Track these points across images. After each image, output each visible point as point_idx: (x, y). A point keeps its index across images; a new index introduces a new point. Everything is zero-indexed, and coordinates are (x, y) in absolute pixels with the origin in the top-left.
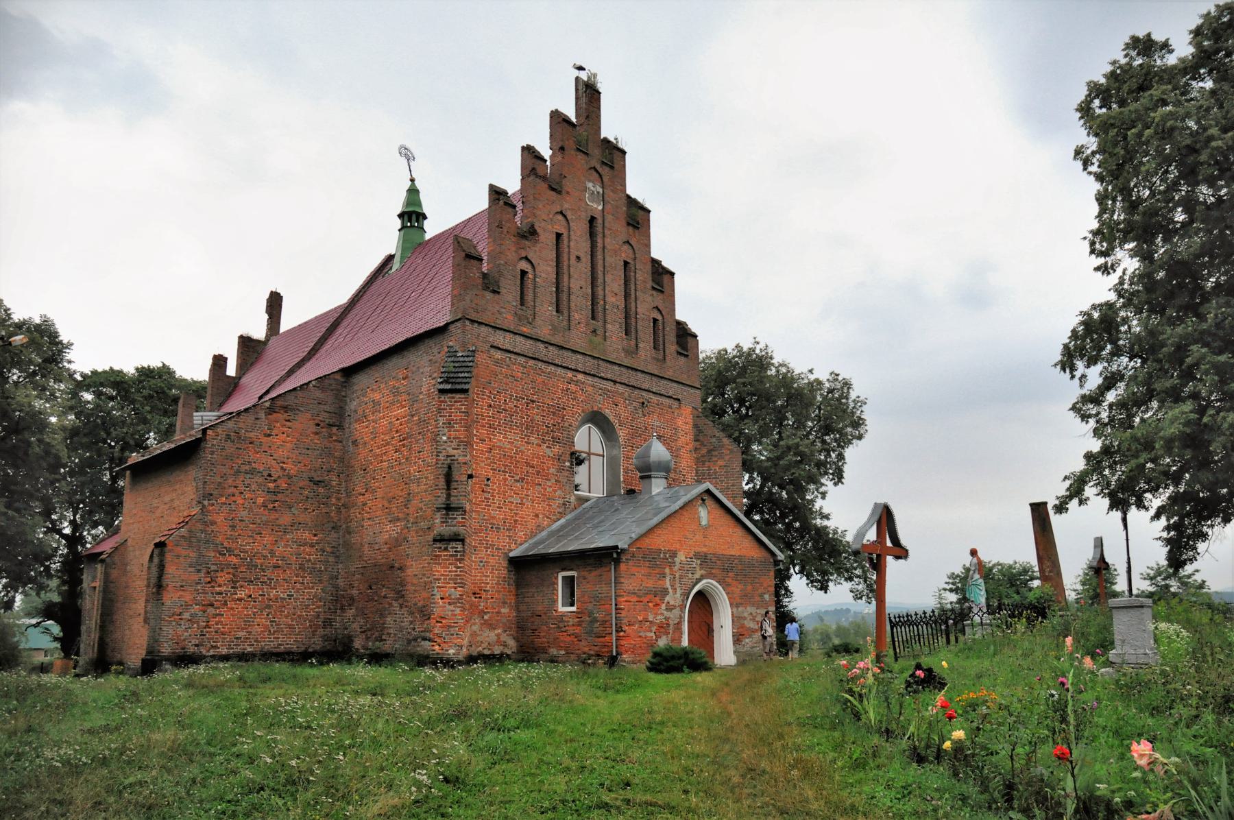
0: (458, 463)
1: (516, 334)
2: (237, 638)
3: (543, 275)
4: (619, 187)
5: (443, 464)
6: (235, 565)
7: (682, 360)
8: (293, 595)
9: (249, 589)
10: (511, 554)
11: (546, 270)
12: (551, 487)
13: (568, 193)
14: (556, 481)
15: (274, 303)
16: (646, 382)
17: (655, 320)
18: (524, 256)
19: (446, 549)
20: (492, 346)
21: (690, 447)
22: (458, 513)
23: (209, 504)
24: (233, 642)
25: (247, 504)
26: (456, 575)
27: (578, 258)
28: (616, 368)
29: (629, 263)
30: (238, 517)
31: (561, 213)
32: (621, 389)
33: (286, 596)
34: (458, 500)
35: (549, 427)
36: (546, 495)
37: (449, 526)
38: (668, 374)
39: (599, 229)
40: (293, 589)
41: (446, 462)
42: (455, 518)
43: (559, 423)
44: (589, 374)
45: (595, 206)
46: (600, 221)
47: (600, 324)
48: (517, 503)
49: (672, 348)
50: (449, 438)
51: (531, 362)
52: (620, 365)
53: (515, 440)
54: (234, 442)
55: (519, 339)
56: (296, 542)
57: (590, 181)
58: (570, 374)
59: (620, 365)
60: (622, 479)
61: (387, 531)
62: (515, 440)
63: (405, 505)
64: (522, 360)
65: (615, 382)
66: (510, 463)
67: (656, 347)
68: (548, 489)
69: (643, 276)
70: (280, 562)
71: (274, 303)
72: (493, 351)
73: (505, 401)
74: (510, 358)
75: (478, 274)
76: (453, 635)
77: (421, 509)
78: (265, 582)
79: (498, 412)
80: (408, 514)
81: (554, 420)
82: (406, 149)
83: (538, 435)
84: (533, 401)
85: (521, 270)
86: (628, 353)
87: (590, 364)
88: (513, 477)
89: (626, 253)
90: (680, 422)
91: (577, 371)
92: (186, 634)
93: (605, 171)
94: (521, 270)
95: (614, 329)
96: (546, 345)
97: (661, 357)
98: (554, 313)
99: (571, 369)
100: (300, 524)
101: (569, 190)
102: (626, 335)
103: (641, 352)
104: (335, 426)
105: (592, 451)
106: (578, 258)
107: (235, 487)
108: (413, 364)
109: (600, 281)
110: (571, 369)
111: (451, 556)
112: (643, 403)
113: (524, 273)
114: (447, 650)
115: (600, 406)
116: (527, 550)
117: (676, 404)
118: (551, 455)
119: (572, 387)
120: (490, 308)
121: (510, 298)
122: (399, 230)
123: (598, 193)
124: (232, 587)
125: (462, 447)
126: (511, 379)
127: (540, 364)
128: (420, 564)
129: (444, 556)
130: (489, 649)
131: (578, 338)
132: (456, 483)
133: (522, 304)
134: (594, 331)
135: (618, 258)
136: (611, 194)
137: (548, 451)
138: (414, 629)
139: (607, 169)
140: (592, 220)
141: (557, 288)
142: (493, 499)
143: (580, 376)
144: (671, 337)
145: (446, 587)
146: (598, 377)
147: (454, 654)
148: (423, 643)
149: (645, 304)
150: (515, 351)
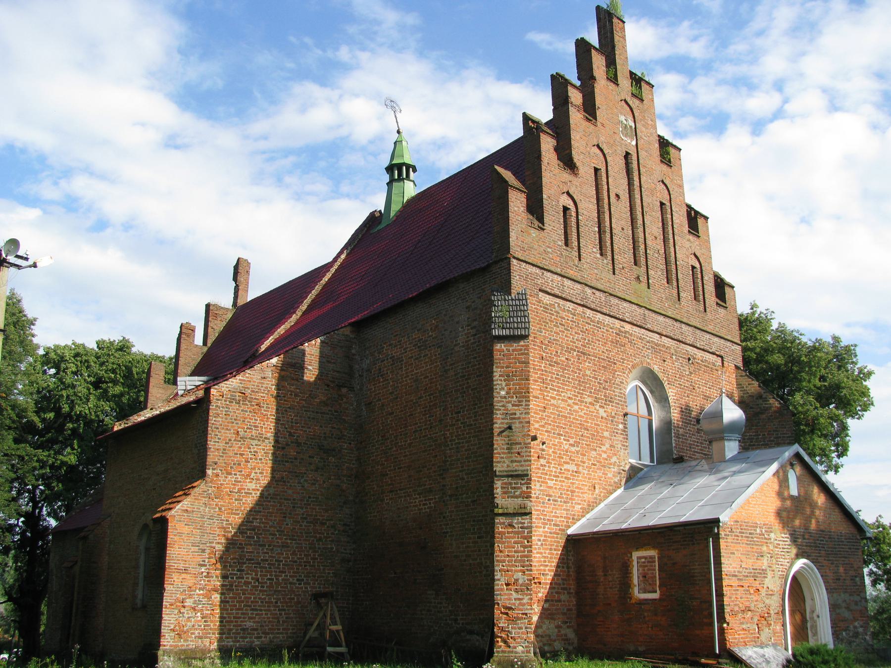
0: (521, 422)
1: (564, 277)
2: (244, 630)
3: (585, 213)
4: (650, 122)
5: (502, 423)
6: (241, 544)
7: (722, 311)
8: (303, 580)
9: (256, 572)
10: (570, 532)
11: (588, 208)
12: (605, 452)
13: (603, 125)
14: (611, 446)
15: (239, 270)
18: (565, 190)
19: (511, 525)
20: (540, 290)
22: (523, 482)
23: (213, 473)
24: (239, 633)
25: (253, 474)
26: (522, 556)
27: (617, 196)
28: (661, 318)
29: (664, 204)
30: (245, 489)
33: (295, 581)
34: (522, 466)
35: (601, 384)
36: (601, 462)
37: (512, 497)
38: (710, 328)
40: (303, 573)
41: (506, 421)
42: (519, 488)
43: (611, 380)
45: (629, 141)
46: (634, 157)
47: (644, 268)
48: (573, 471)
49: (711, 298)
50: (507, 393)
51: (580, 309)
52: (665, 316)
54: (239, 403)
55: (568, 283)
56: (306, 518)
57: (621, 114)
59: (665, 316)
60: (674, 445)
61: (416, 506)
63: (442, 475)
65: (660, 334)
66: (565, 424)
67: (696, 298)
68: (604, 456)
69: (680, 219)
70: (289, 541)
71: (239, 270)
72: (541, 294)
73: (557, 352)
75: (522, 209)
76: (521, 628)
77: (463, 479)
78: (274, 564)
79: (550, 365)
80: (444, 486)
81: (606, 376)
82: (391, 101)
83: (591, 392)
87: (637, 313)
88: (568, 441)
92: (189, 624)
93: (635, 103)
95: (656, 276)
96: (594, 291)
97: (702, 308)
98: (598, 256)
100: (310, 497)
101: (604, 122)
102: (668, 283)
103: (683, 302)
104: (345, 387)
105: (640, 413)
106: (617, 196)
107: (242, 455)
108: (444, 313)
109: (640, 222)
111: (518, 533)
114: (515, 647)
115: (648, 361)
116: (582, 526)
118: (605, 415)
120: (536, 247)
121: (555, 237)
122: (387, 184)
123: (631, 127)
124: (238, 570)
125: (524, 403)
126: (561, 328)
127: (588, 312)
128: (463, 543)
129: (508, 532)
130: (550, 645)
131: (622, 284)
132: (518, 446)
133: (566, 244)
134: (638, 278)
135: (655, 198)
136: (644, 129)
137: (601, 411)
138: (456, 620)
139: (637, 102)
140: (627, 156)
141: (599, 227)
142: (549, 467)
144: (710, 288)
145: (511, 571)
146: (644, 328)
147: (523, 652)
148: (468, 637)
150: (563, 296)
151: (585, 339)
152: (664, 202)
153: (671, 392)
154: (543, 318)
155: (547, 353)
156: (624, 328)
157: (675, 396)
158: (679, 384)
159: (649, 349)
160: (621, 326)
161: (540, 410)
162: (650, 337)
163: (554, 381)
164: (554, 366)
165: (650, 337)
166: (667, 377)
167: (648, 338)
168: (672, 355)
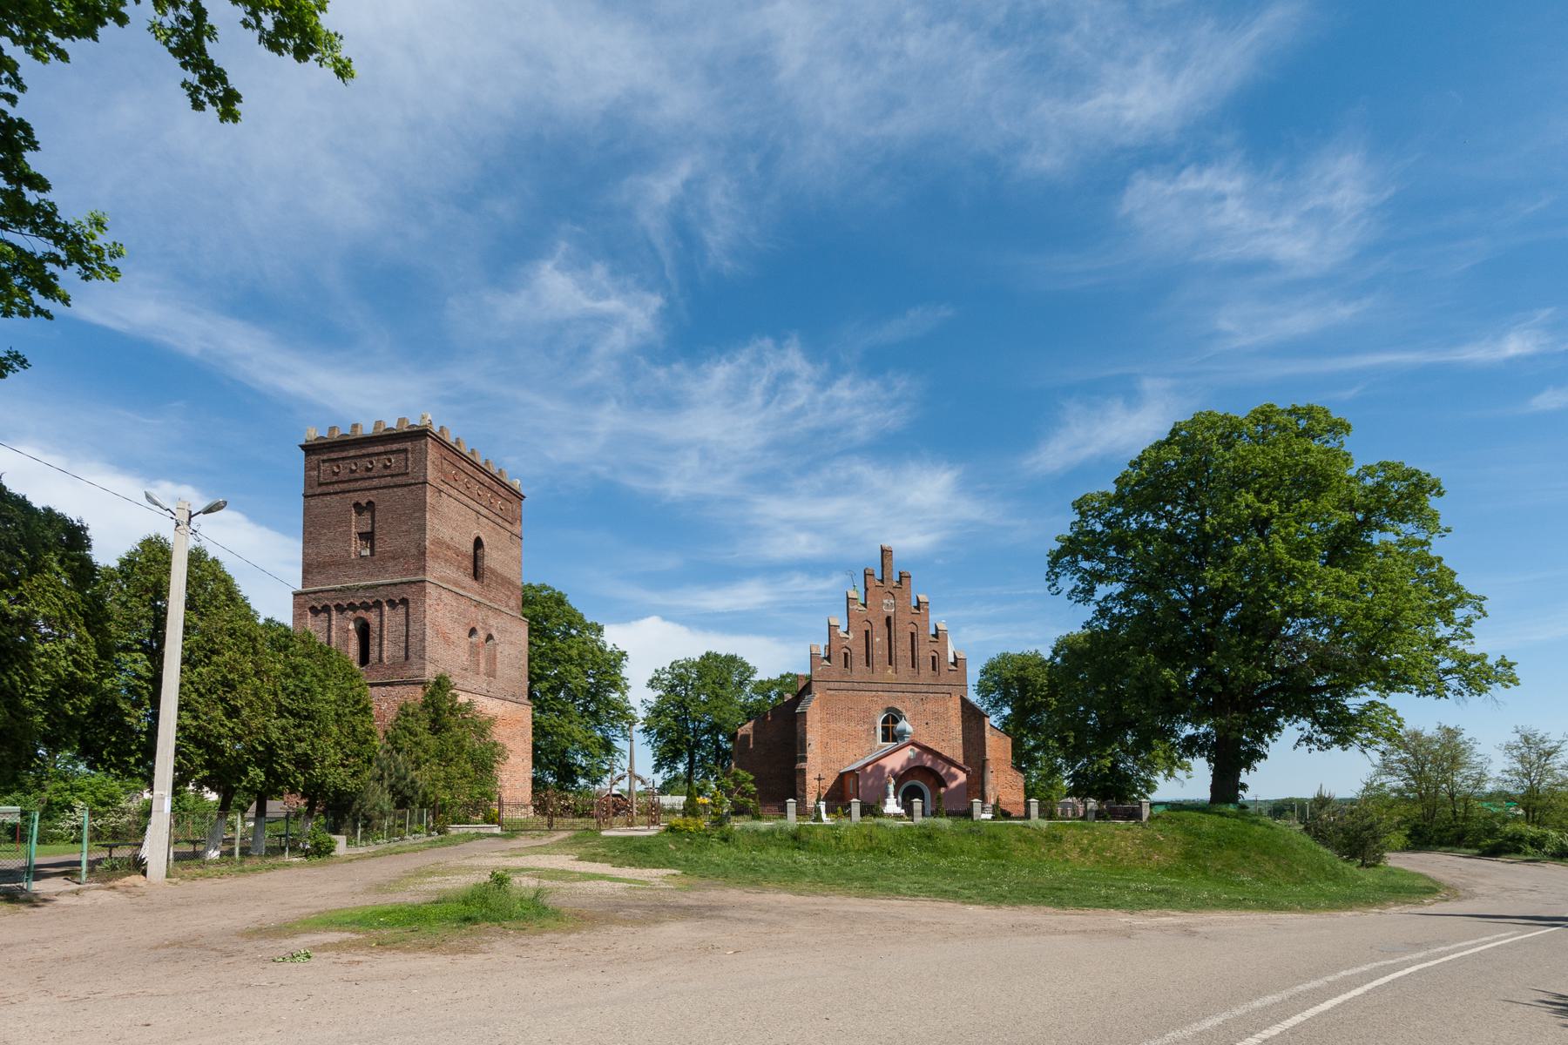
16: (925, 689)
17: (933, 658)
31: (867, 621)
39: (893, 621)
67: (934, 669)
86: (911, 677)
89: (912, 628)
90: (950, 704)
113: (846, 654)
140: (888, 619)
149: (925, 652)
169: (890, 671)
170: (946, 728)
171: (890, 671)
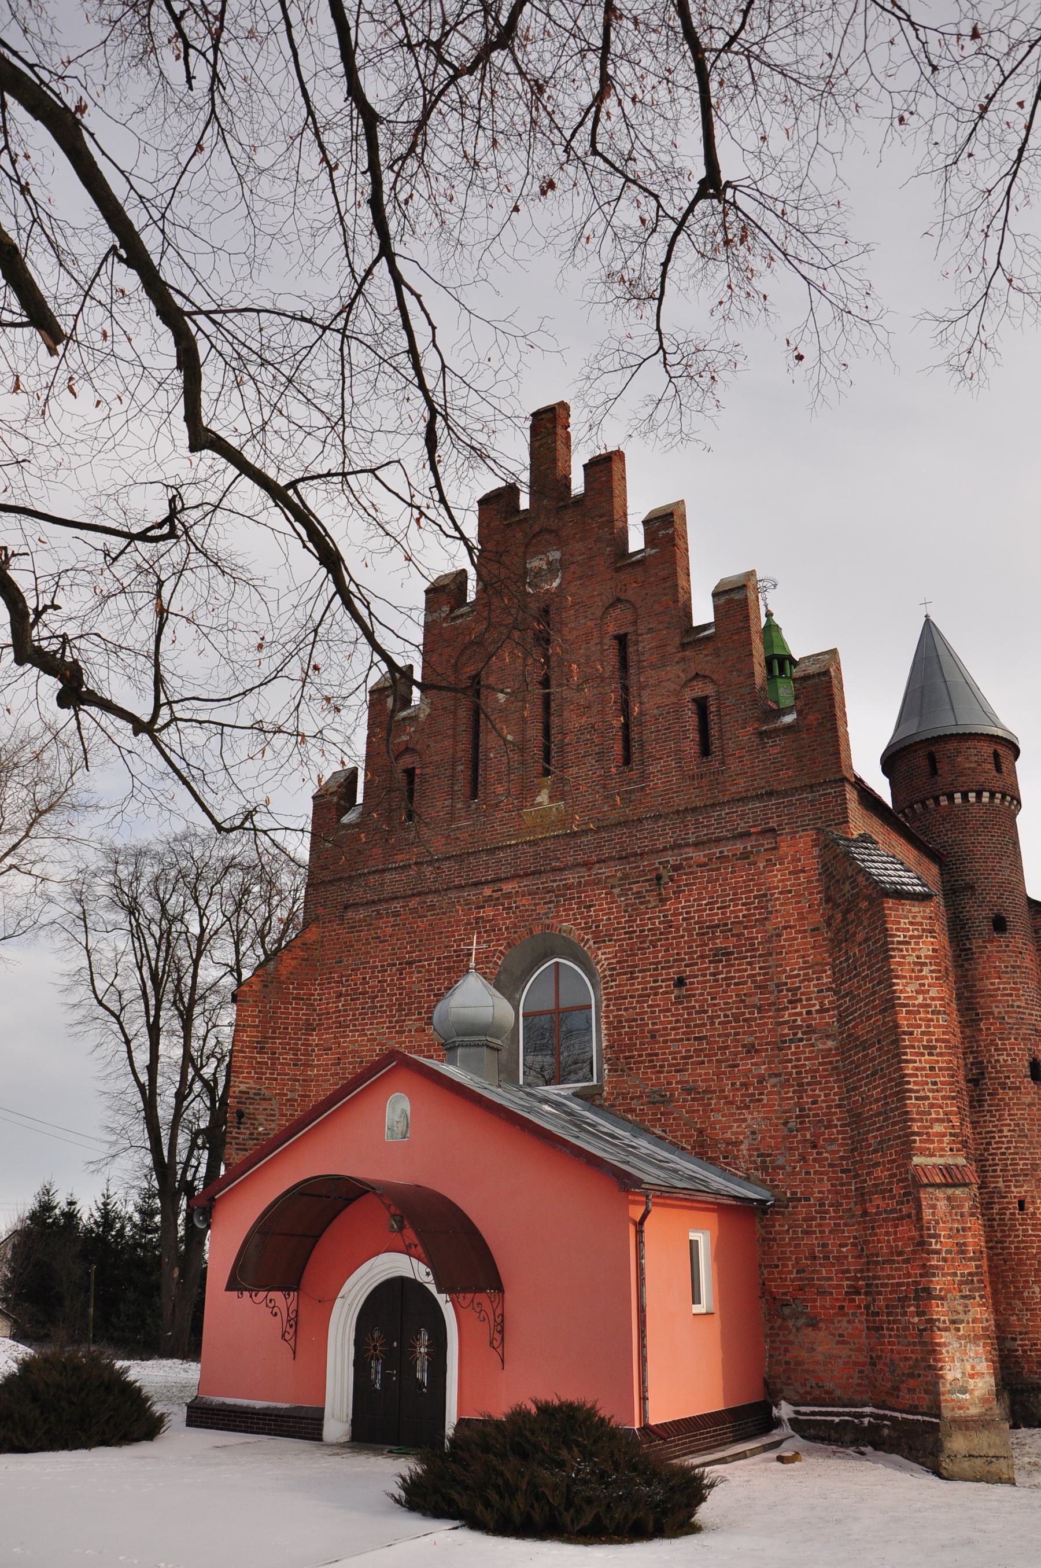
21: (817, 918)
32: (605, 871)
44: (527, 875)
51: (413, 903)
53: (379, 1034)
58: (487, 891)
62: (379, 1034)
64: (397, 905)
65: (588, 865)
72: (350, 914)
73: (364, 978)
74: (378, 911)
83: (420, 1013)
84: (410, 963)
85: (405, 771)
91: (500, 880)
94: (405, 771)
99: (487, 882)
110: (487, 882)
112: (659, 878)
115: (547, 922)
117: (767, 843)
119: (488, 912)
127: (429, 899)
143: (508, 887)
146: (545, 871)
151: (415, 941)
152: (622, 632)
153: (603, 954)
154: (345, 943)
155: (350, 985)
156: (501, 890)
157: (615, 957)
158: (625, 933)
159: (551, 902)
160: (493, 891)
161: (332, 1065)
162: (561, 880)
163: (357, 1019)
164: (358, 999)
165: (561, 880)
166: (592, 933)
167: (555, 884)
168: (613, 887)
169: (543, 798)
170: (762, 988)
171: (543, 798)
